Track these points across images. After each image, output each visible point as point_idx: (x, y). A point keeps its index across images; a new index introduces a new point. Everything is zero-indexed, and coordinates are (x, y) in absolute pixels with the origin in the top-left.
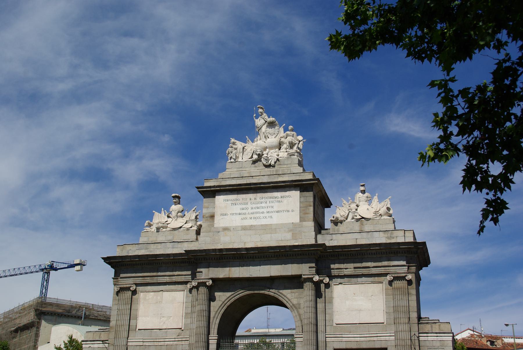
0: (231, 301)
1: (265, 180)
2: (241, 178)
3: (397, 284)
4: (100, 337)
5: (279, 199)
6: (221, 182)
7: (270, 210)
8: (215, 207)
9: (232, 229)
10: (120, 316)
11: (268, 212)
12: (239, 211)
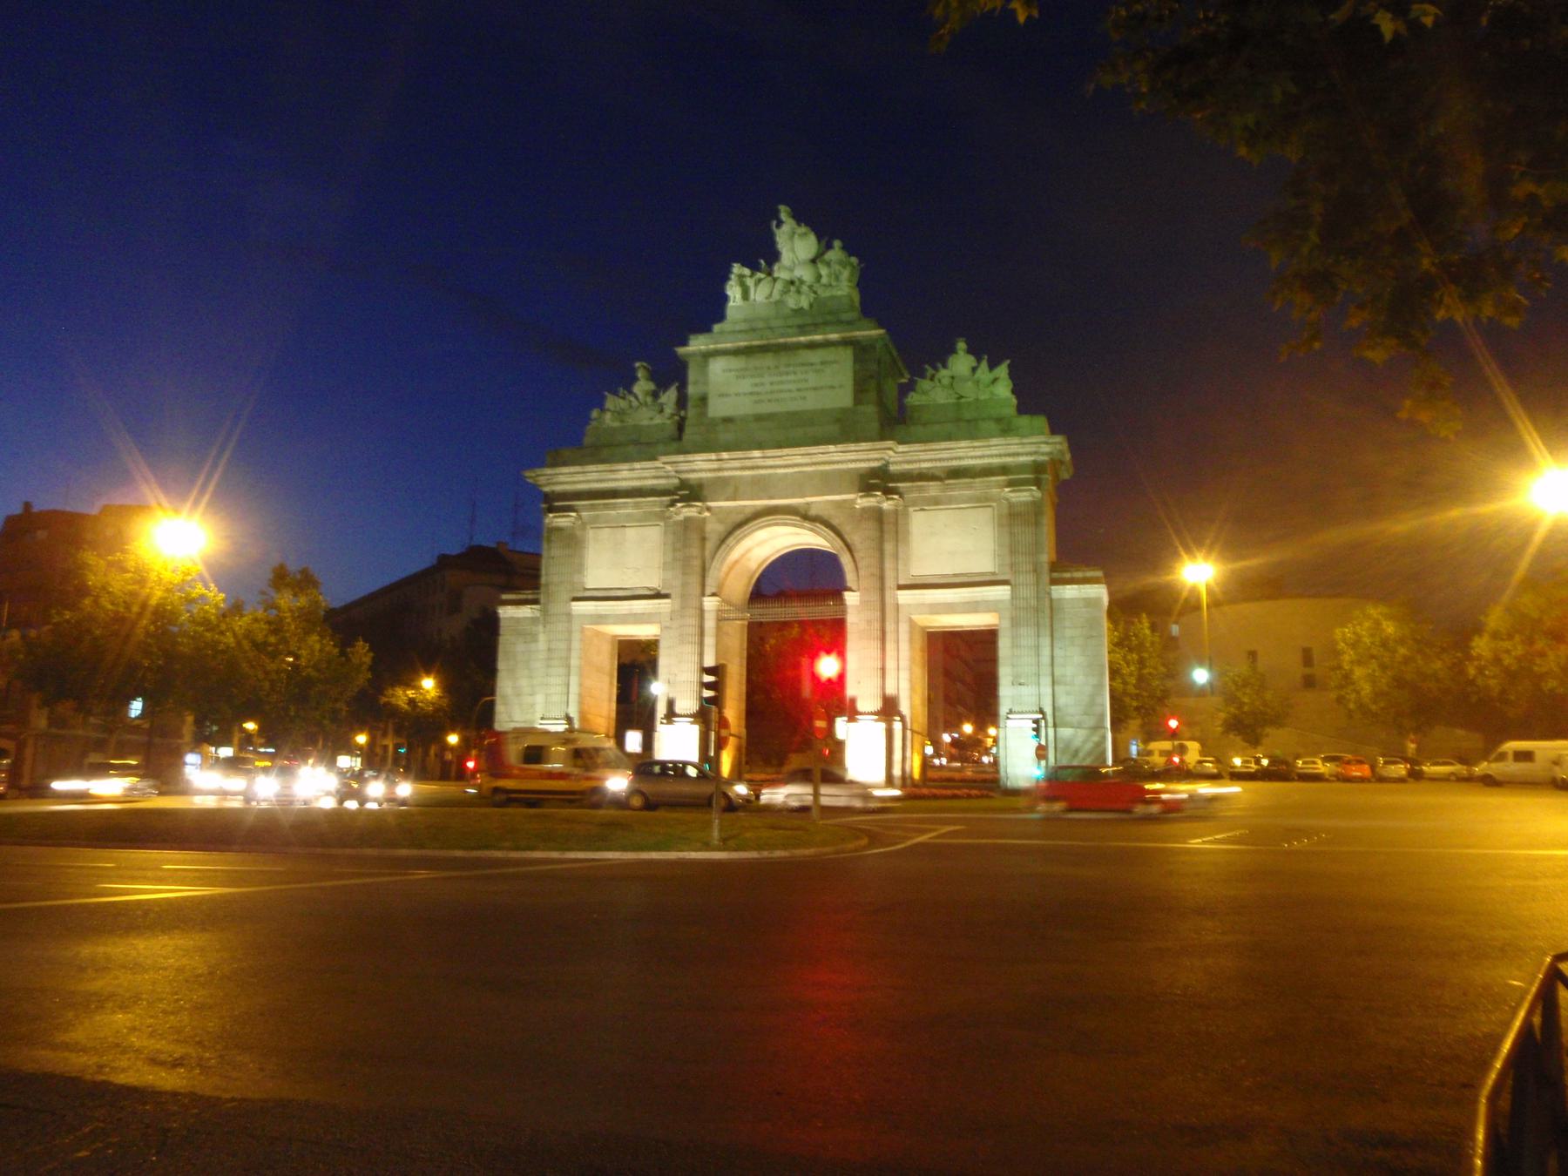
5: (819, 367)
11: (799, 390)
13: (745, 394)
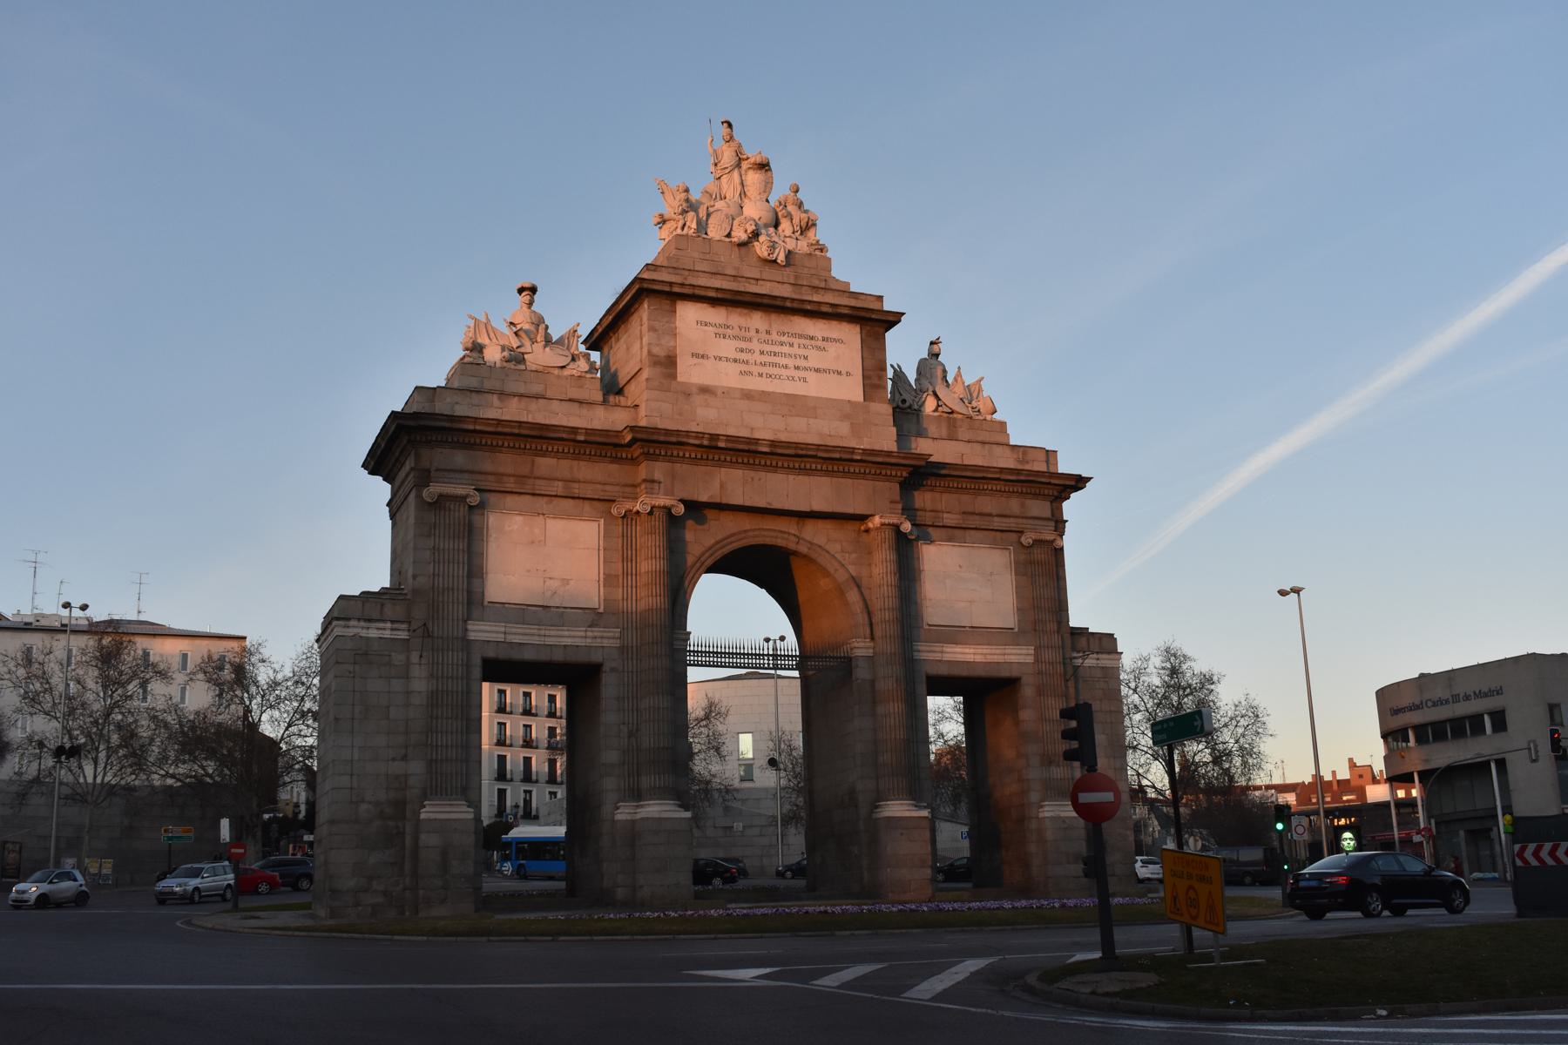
0: (716, 555)
1: (785, 291)
2: (732, 279)
3: (1040, 554)
4: (381, 613)
5: (820, 343)
6: (685, 279)
7: (802, 363)
8: (676, 335)
9: (719, 393)
10: (441, 565)
11: (797, 368)
13: (727, 360)
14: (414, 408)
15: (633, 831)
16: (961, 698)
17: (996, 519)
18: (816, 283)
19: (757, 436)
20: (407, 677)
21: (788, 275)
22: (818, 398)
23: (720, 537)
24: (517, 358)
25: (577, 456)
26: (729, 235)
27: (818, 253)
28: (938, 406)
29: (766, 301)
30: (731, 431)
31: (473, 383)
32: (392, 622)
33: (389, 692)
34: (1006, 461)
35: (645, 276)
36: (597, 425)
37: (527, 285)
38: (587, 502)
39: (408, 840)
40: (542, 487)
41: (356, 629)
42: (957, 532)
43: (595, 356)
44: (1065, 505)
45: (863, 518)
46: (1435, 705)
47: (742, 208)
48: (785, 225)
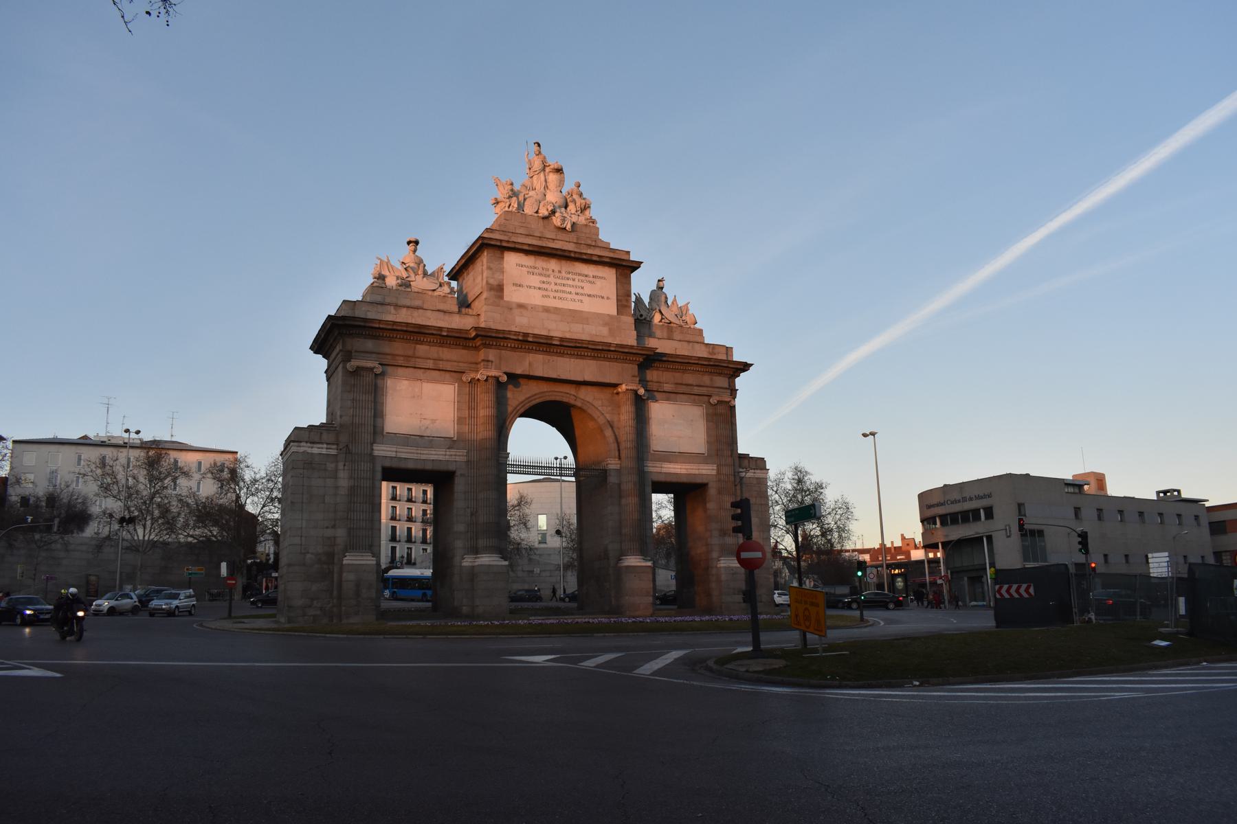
3: (721, 409)
4: (320, 439)
5: (591, 279)
7: (580, 291)
9: (530, 308)
11: (577, 294)
12: (538, 285)
13: (535, 288)
14: (342, 314)
15: (473, 573)
16: (673, 495)
17: (695, 388)
18: (589, 242)
19: (552, 334)
20: (336, 478)
21: (572, 237)
22: (589, 312)
23: (528, 396)
24: (405, 284)
25: (442, 345)
26: (537, 212)
27: (591, 224)
28: (662, 319)
29: (559, 253)
30: (536, 332)
31: (379, 298)
32: (327, 444)
33: (325, 487)
34: (701, 353)
35: (486, 235)
36: (454, 326)
37: (413, 239)
38: (447, 373)
39: (336, 576)
40: (420, 363)
41: (304, 448)
42: (673, 395)
43: (454, 284)
44: (737, 380)
45: (615, 386)
46: (952, 503)
47: (545, 195)
48: (571, 207)
